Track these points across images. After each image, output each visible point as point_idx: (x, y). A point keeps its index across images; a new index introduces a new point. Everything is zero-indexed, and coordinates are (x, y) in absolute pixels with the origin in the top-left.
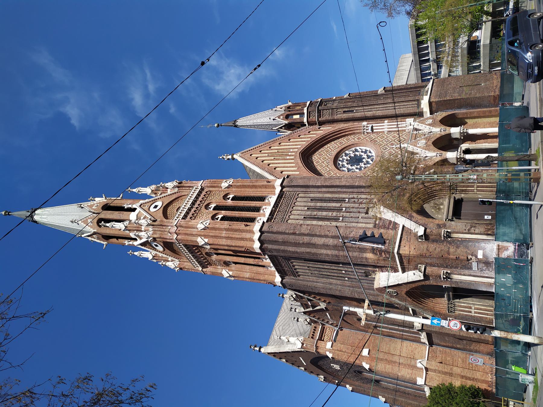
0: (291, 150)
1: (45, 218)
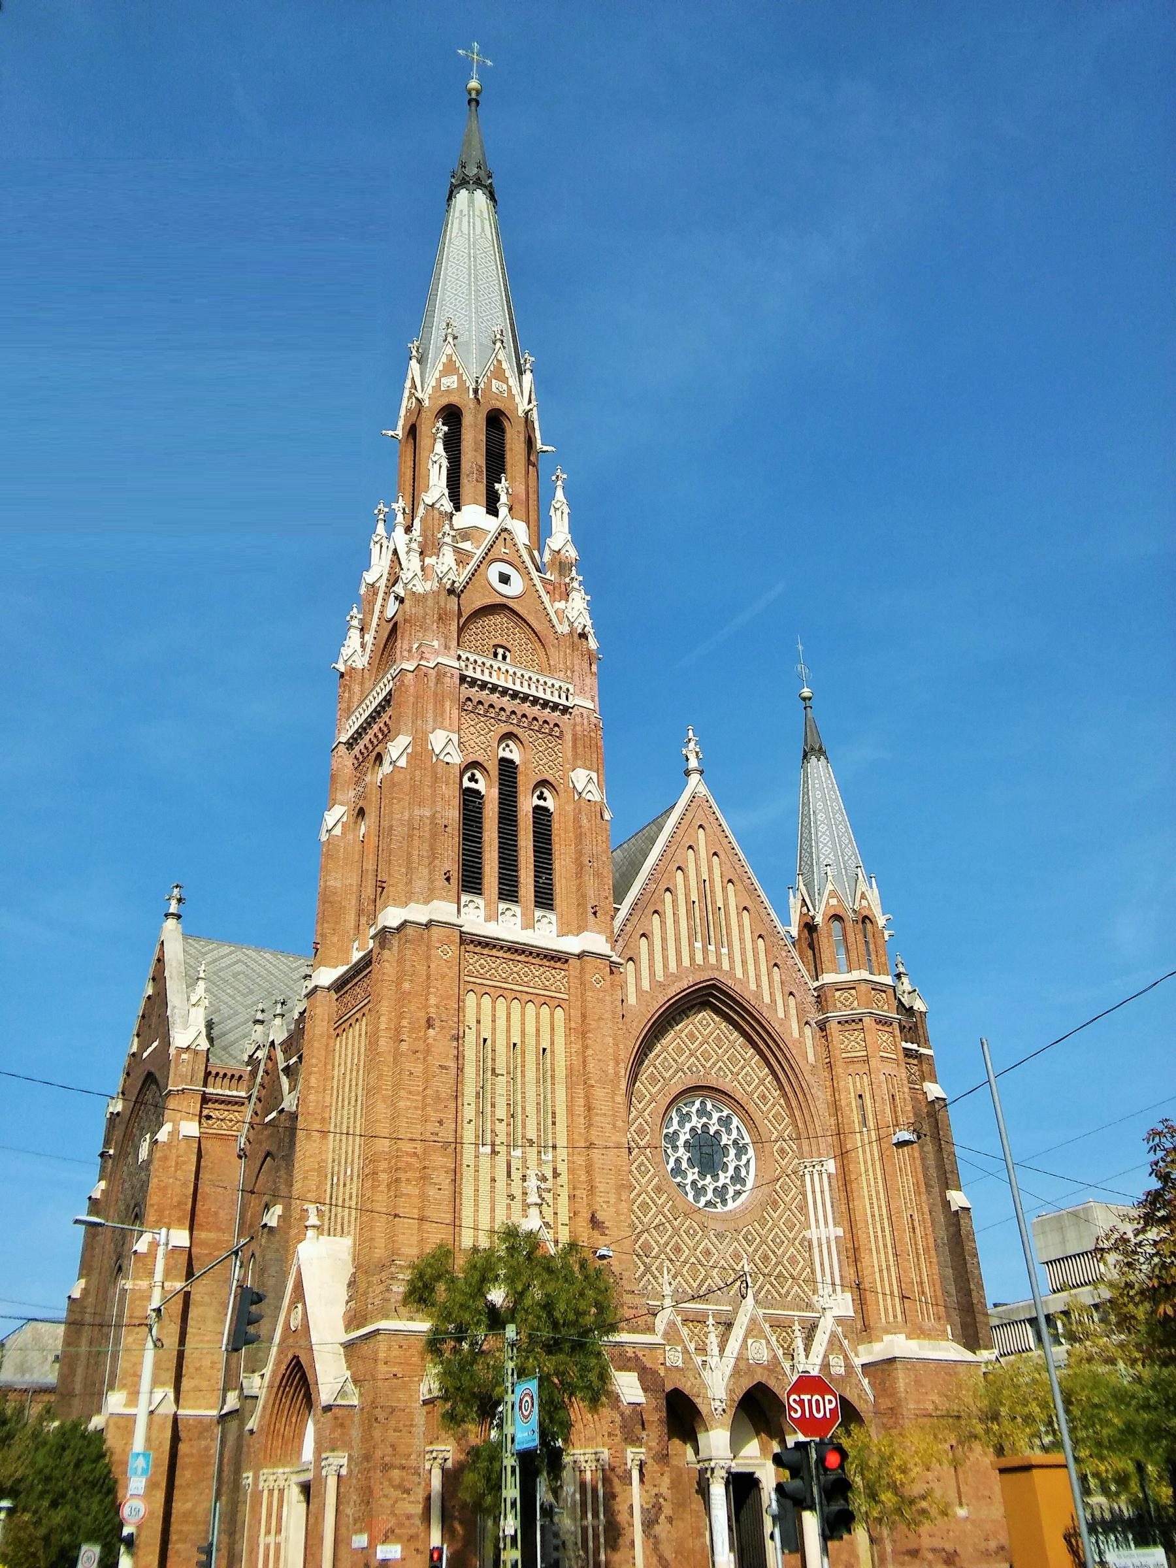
0: (724, 951)
1: (460, 229)
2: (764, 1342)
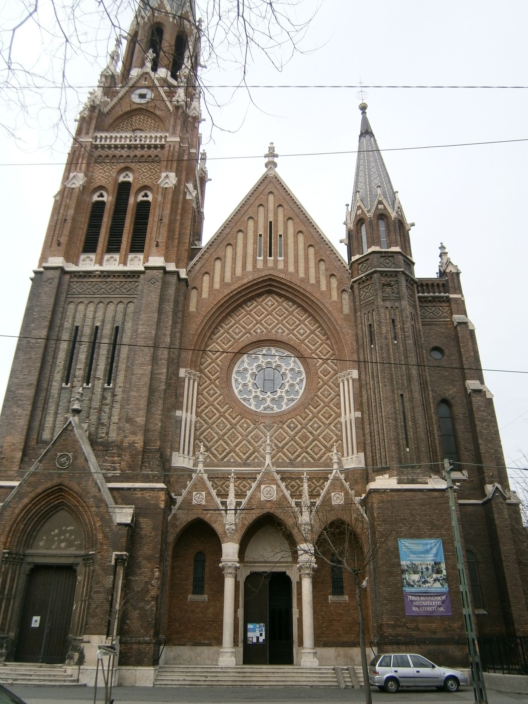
2: (274, 487)
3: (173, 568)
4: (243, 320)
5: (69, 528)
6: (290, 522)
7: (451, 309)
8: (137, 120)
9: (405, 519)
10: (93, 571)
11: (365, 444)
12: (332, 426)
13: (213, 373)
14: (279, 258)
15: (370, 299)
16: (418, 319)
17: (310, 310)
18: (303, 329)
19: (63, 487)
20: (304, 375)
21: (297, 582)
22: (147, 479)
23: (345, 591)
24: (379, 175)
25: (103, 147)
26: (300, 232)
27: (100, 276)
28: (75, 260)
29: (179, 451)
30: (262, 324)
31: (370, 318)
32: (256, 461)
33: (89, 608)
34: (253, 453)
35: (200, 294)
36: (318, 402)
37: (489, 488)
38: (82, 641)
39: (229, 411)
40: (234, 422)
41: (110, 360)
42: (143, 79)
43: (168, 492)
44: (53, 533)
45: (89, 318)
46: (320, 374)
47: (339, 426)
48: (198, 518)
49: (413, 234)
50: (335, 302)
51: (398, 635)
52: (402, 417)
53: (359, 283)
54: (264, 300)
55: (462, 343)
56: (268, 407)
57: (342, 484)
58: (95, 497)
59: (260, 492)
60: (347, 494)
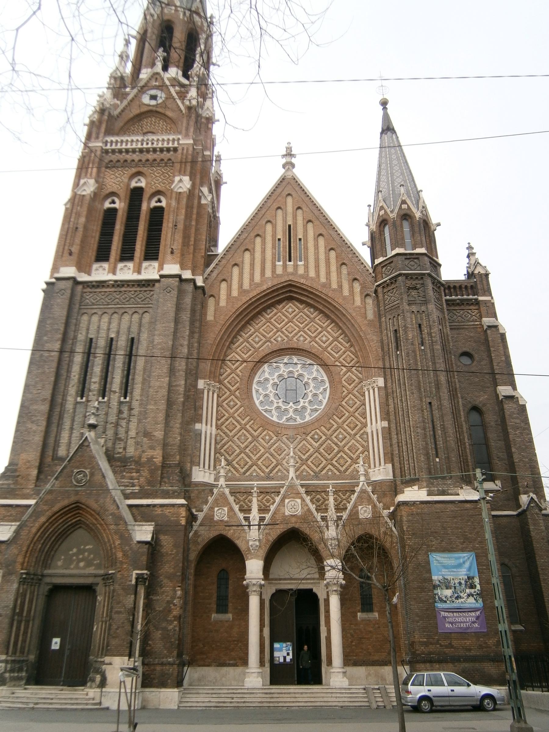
2: (299, 501)
3: (195, 587)
4: (263, 328)
5: (87, 547)
6: (315, 537)
7: (480, 312)
8: (147, 123)
9: (436, 532)
10: (114, 591)
11: (392, 454)
12: (357, 437)
13: (233, 384)
14: (299, 263)
15: (395, 303)
16: (445, 323)
17: (333, 317)
18: (326, 336)
19: (80, 505)
20: (327, 385)
21: (324, 599)
22: (166, 495)
23: (375, 609)
24: (402, 174)
25: (113, 151)
26: (321, 235)
27: (113, 286)
28: (87, 270)
29: (199, 466)
30: (282, 332)
31: (395, 323)
32: (279, 474)
33: (109, 629)
34: (276, 466)
35: (217, 302)
36: (341, 411)
37: (524, 499)
38: (103, 663)
39: (251, 423)
40: (256, 434)
41: (126, 372)
42: (154, 80)
43: (188, 508)
44: (71, 552)
45: (104, 330)
46: (344, 382)
47: (365, 436)
48: (221, 535)
49: (438, 234)
50: (359, 307)
51: (430, 653)
52: (431, 426)
53: (383, 287)
54: (284, 307)
55: (493, 347)
56: (291, 418)
57: (370, 496)
58: (113, 514)
59: (284, 506)
60: (374, 506)
